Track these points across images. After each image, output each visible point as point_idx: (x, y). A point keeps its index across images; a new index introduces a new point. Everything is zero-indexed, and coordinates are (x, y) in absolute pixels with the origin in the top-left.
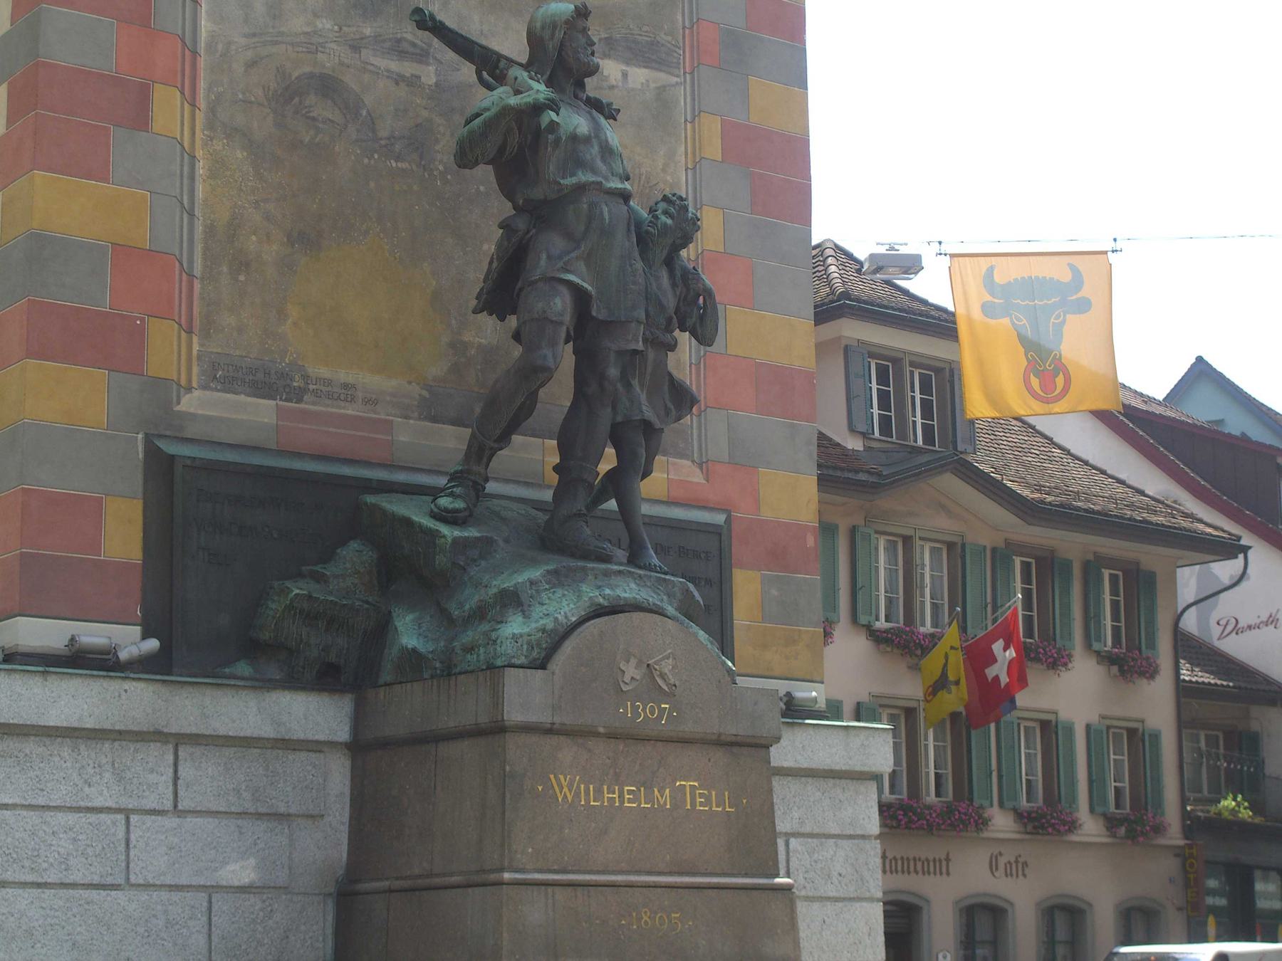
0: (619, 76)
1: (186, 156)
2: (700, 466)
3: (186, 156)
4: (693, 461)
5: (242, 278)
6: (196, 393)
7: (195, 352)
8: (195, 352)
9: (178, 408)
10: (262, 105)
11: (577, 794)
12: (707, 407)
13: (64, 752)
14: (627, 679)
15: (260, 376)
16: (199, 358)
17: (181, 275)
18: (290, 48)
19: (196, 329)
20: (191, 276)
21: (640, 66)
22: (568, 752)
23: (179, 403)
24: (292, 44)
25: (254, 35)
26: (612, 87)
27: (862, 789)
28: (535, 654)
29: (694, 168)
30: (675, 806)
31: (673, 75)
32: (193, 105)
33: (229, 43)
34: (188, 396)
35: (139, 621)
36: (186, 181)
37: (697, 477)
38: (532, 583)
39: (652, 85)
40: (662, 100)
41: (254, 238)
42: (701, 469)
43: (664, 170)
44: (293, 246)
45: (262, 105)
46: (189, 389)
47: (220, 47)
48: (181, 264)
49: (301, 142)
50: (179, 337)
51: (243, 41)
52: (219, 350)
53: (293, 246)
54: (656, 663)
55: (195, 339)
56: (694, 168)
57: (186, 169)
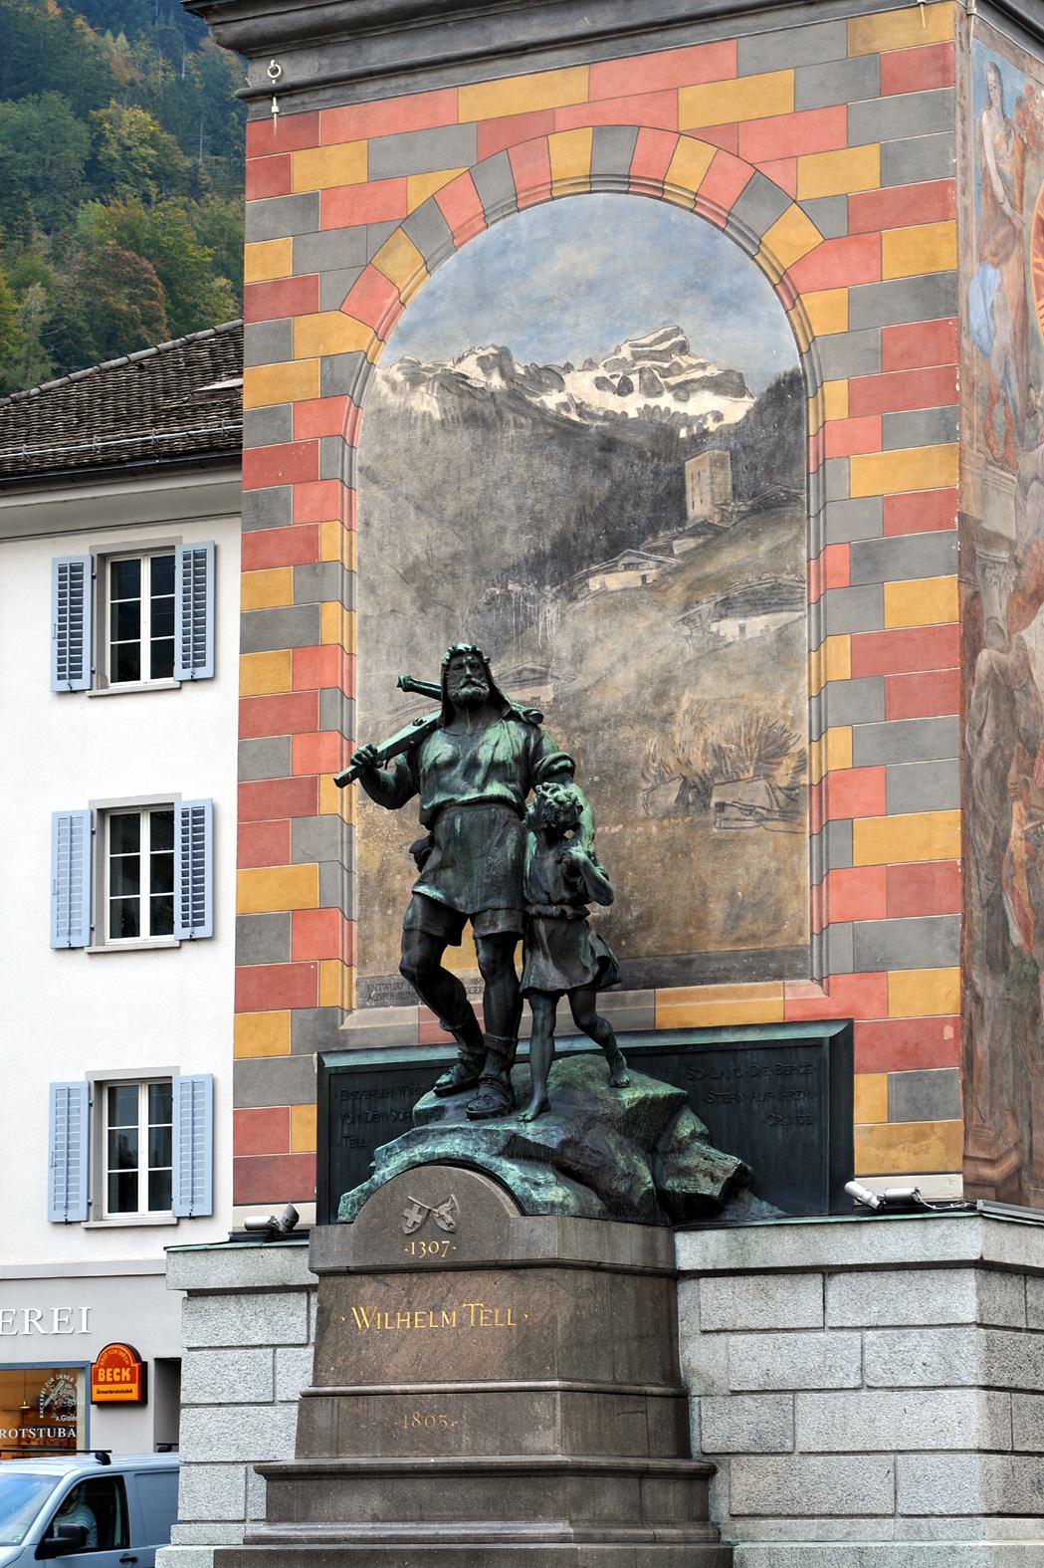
4: (812, 979)
5: (390, 912)
7: (354, 981)
8: (354, 981)
13: (231, 1302)
16: (358, 984)
19: (355, 962)
20: (350, 920)
21: (759, 615)
25: (397, 710)
27: (956, 1277)
29: (819, 695)
31: (796, 611)
33: (378, 723)
35: (315, 1198)
37: (817, 992)
39: (773, 629)
40: (784, 639)
41: (399, 877)
42: (822, 985)
43: (784, 706)
46: (350, 1011)
47: (370, 729)
51: (388, 718)
52: (373, 974)
55: (355, 970)
56: (819, 695)
57: (345, 836)
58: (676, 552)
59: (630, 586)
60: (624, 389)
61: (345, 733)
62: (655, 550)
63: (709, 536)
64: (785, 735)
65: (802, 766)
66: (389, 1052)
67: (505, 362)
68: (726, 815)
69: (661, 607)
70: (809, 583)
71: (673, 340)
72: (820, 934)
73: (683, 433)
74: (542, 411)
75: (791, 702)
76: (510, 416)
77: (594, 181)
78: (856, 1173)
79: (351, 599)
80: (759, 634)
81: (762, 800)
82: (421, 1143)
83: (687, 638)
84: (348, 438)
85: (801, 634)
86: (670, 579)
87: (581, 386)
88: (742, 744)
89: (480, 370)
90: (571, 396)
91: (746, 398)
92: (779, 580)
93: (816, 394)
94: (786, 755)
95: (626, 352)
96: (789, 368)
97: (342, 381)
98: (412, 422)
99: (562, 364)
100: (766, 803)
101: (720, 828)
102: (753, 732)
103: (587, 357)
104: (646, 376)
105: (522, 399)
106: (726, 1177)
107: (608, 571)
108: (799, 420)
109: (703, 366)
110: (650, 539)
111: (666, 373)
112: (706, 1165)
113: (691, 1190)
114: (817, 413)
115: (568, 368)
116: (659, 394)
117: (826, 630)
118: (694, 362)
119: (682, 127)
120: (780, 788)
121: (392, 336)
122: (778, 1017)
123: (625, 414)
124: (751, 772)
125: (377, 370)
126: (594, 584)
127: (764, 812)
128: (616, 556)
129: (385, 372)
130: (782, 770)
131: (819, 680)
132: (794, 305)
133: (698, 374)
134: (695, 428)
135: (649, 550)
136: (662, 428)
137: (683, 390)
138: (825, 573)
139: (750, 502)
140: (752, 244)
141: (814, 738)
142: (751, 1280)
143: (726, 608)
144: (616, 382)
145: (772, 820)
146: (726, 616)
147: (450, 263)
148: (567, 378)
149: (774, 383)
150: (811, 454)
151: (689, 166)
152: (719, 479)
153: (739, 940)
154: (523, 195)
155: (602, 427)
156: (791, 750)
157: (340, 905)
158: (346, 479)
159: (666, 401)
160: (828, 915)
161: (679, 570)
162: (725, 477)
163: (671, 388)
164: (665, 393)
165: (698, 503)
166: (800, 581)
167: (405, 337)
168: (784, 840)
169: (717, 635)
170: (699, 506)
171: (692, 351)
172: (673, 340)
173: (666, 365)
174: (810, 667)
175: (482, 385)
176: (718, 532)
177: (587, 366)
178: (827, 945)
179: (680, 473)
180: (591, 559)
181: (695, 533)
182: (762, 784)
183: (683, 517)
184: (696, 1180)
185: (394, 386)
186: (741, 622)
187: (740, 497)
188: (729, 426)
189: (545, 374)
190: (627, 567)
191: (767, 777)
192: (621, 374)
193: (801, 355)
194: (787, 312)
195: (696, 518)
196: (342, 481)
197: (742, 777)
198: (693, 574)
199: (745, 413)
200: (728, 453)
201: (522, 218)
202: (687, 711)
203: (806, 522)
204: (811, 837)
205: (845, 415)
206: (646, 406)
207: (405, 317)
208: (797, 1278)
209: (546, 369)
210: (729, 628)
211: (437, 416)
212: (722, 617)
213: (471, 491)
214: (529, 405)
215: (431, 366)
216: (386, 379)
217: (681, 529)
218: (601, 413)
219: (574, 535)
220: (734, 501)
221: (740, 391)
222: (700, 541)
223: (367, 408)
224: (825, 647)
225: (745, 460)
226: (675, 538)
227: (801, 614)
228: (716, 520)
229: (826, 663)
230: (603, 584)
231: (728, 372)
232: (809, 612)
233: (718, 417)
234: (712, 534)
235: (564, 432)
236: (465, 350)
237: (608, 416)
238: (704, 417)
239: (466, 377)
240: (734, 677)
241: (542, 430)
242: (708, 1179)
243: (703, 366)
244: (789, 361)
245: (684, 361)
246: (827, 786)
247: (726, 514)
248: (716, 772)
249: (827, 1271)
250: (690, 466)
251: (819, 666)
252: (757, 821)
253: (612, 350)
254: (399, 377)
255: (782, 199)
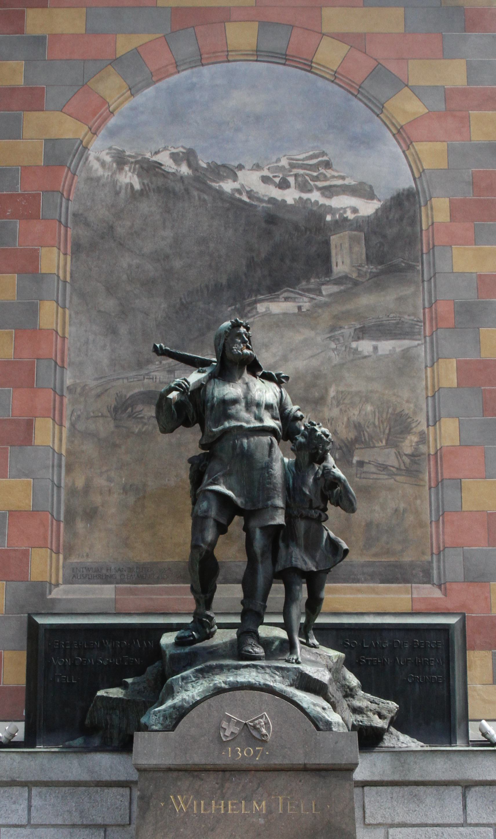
0: (371, 349)
1: (56, 455)
2: (439, 586)
3: (56, 455)
4: (433, 584)
6: (62, 587)
9: (49, 597)
10: (106, 417)
11: (191, 807)
12: (445, 548)
14: (227, 733)
15: (104, 571)
17: (52, 522)
18: (125, 381)
19: (61, 551)
20: (58, 521)
21: (387, 340)
22: (185, 783)
23: (50, 593)
24: (127, 378)
25: (101, 378)
26: (365, 357)
28: (168, 722)
29: (433, 396)
30: (270, 812)
31: (416, 340)
32: (61, 425)
34: (56, 589)
35: (24, 719)
36: (55, 469)
37: (437, 594)
38: (183, 678)
39: (398, 350)
40: (407, 356)
44: (126, 493)
45: (106, 417)
46: (57, 585)
48: (53, 516)
49: (133, 433)
50: (51, 557)
53: (126, 493)
54: (251, 722)
56: (433, 396)
58: (324, 293)
59: (289, 312)
60: (284, 185)
61: (58, 391)
62: (309, 291)
63: (350, 286)
64: (409, 420)
65: (423, 439)
66: (91, 617)
67: (191, 158)
68: (365, 469)
69: (312, 329)
70: (425, 324)
71: (320, 159)
72: (439, 554)
73: (329, 218)
74: (220, 193)
75: (411, 398)
76: (195, 193)
77: (259, 55)
78: (469, 718)
79: (64, 300)
80: (387, 353)
81: (392, 461)
82: (217, 674)
83: (333, 350)
84: (65, 194)
85: (419, 356)
86: (320, 311)
87: (250, 180)
88: (377, 423)
89: (171, 161)
90: (243, 186)
91: (375, 201)
92: (402, 319)
93: (426, 205)
94: (409, 433)
95: (284, 162)
96: (407, 186)
97: (62, 155)
98: (118, 188)
99: (236, 164)
100: (396, 464)
101: (360, 478)
102: (384, 416)
103: (255, 162)
104: (300, 179)
105: (205, 183)
106: (390, 716)
107: (272, 300)
108: (414, 221)
109: (343, 178)
110: (304, 283)
111: (316, 179)
112: (374, 706)
113: (366, 723)
114: (427, 216)
115: (241, 167)
116: (310, 191)
117: (437, 354)
118: (336, 174)
119: (324, 31)
120: (406, 455)
121: (103, 132)
122: (408, 608)
123: (284, 201)
124: (384, 442)
125: (89, 152)
126: (261, 308)
127: (394, 470)
128: (277, 291)
129: (97, 155)
130: (407, 442)
131: (433, 386)
132: (408, 148)
133: (340, 182)
134: (337, 216)
135: (303, 290)
136: (312, 213)
137: (329, 191)
138: (436, 318)
139: (379, 267)
140: (378, 108)
141: (431, 423)
142: (406, 789)
143: (362, 333)
144: (277, 180)
145: (400, 475)
146: (363, 339)
147: (150, 91)
148: (239, 174)
149: (395, 194)
150: (424, 241)
151: (330, 54)
152: (356, 249)
153: (375, 555)
154: (206, 56)
155: (267, 207)
156: (414, 430)
157: (50, 510)
158: (63, 220)
159: (315, 196)
160: (444, 542)
161: (326, 305)
162: (361, 250)
163: (319, 189)
164: (315, 191)
165: (340, 263)
166: (418, 321)
167: (113, 133)
168: (410, 490)
169: (356, 349)
170: (342, 264)
171: (334, 167)
172: (320, 159)
173: (315, 174)
174: (426, 377)
175: (173, 171)
176: (356, 283)
177: (255, 167)
178: (444, 562)
179: (327, 243)
180: (258, 292)
181: (339, 281)
182: (393, 450)
183: (329, 271)
184: (368, 717)
185: (103, 164)
186: (374, 343)
187: (372, 263)
188: (363, 217)
189: (222, 169)
190: (286, 299)
191: (396, 446)
192: (281, 176)
193: (415, 179)
194: (404, 152)
195: (340, 272)
196: (60, 222)
197: (376, 445)
198: (337, 309)
199: (374, 211)
200: (362, 235)
201: (206, 71)
202: (334, 397)
203: (421, 284)
204: (430, 488)
205: (448, 219)
206: (300, 198)
207: (112, 122)
208: (442, 788)
209: (224, 166)
210: (365, 346)
211: (137, 186)
212: (359, 339)
213: (163, 238)
214: (210, 187)
215: (133, 154)
216: (98, 159)
217: (328, 279)
218: (266, 199)
219: (245, 274)
220: (367, 264)
221: (370, 196)
222: (342, 288)
223: (82, 175)
224: (438, 365)
225: (375, 240)
226: (323, 284)
227: (420, 342)
228: (354, 276)
229: (438, 375)
230: (268, 308)
231: (362, 183)
232: (425, 342)
233: (355, 210)
234: (351, 285)
235: (236, 208)
236: (161, 146)
237: (272, 200)
238: (345, 210)
239: (161, 165)
240: (370, 379)
241: (220, 204)
242: (376, 717)
243: (343, 178)
244: (405, 182)
245: (329, 173)
246: (441, 456)
247: (361, 272)
248: (357, 440)
249: (467, 786)
250: (334, 239)
251: (433, 378)
252: (389, 475)
253: (274, 160)
254: (108, 159)
255: (399, 84)
